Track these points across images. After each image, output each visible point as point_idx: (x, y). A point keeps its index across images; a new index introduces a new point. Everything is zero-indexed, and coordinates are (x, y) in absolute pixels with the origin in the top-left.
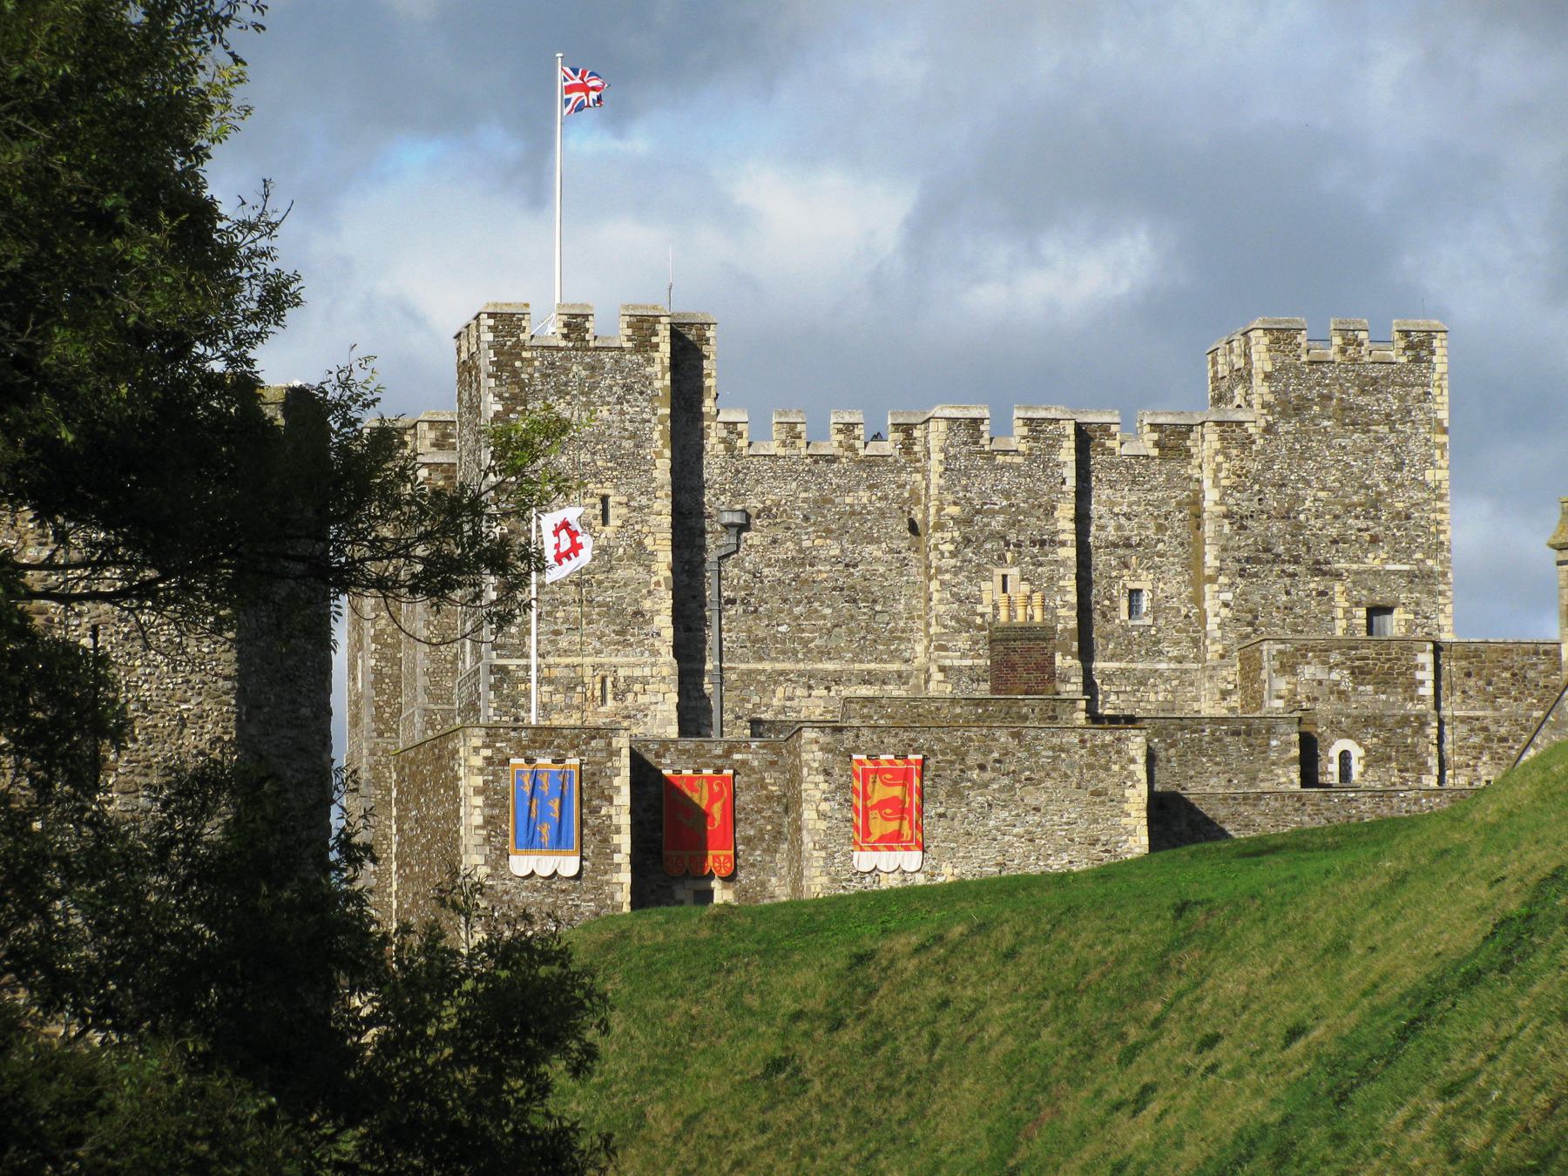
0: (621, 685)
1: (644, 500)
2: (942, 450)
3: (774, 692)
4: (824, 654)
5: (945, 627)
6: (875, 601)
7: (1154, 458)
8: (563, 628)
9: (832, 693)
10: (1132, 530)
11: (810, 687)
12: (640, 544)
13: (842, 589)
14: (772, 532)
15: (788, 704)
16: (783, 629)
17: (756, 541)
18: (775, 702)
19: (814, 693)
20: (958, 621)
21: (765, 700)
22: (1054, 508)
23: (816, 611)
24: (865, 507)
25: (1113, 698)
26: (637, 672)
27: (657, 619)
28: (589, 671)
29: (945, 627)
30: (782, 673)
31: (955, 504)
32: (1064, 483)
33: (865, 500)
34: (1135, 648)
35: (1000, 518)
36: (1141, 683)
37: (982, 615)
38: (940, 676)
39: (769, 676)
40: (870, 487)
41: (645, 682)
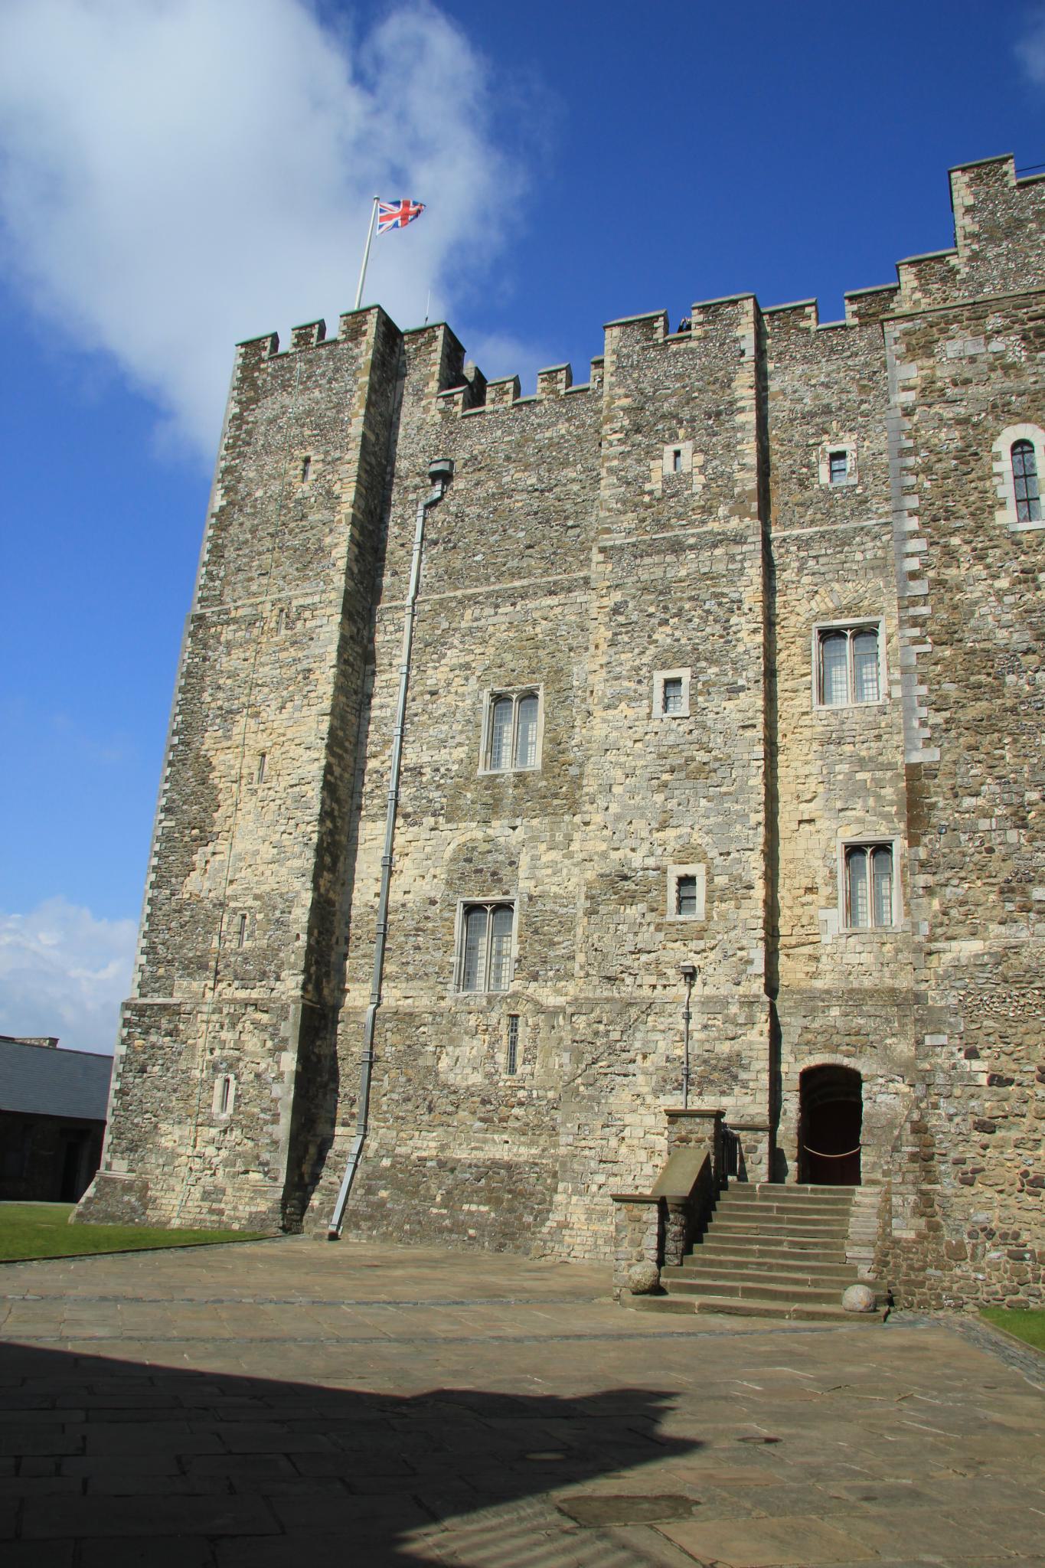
0: (293, 616)
1: (337, 454)
2: (614, 352)
3: (462, 616)
4: (516, 574)
5: (610, 510)
6: (567, 518)
7: (853, 328)
8: (255, 574)
9: (518, 608)
10: (830, 398)
11: (497, 606)
12: (329, 492)
13: (536, 513)
14: (476, 476)
15: (475, 624)
16: (478, 558)
17: (461, 486)
18: (463, 625)
19: (500, 611)
20: (624, 503)
21: (453, 625)
22: (731, 380)
23: (510, 537)
24: (563, 436)
25: (811, 563)
26: (309, 601)
27: (334, 554)
28: (268, 606)
29: (610, 510)
30: (469, 598)
31: (627, 396)
32: (743, 353)
33: (563, 432)
34: (839, 510)
35: (673, 400)
36: (844, 544)
37: (651, 493)
38: (601, 557)
39: (460, 602)
40: (568, 420)
41: (312, 607)
